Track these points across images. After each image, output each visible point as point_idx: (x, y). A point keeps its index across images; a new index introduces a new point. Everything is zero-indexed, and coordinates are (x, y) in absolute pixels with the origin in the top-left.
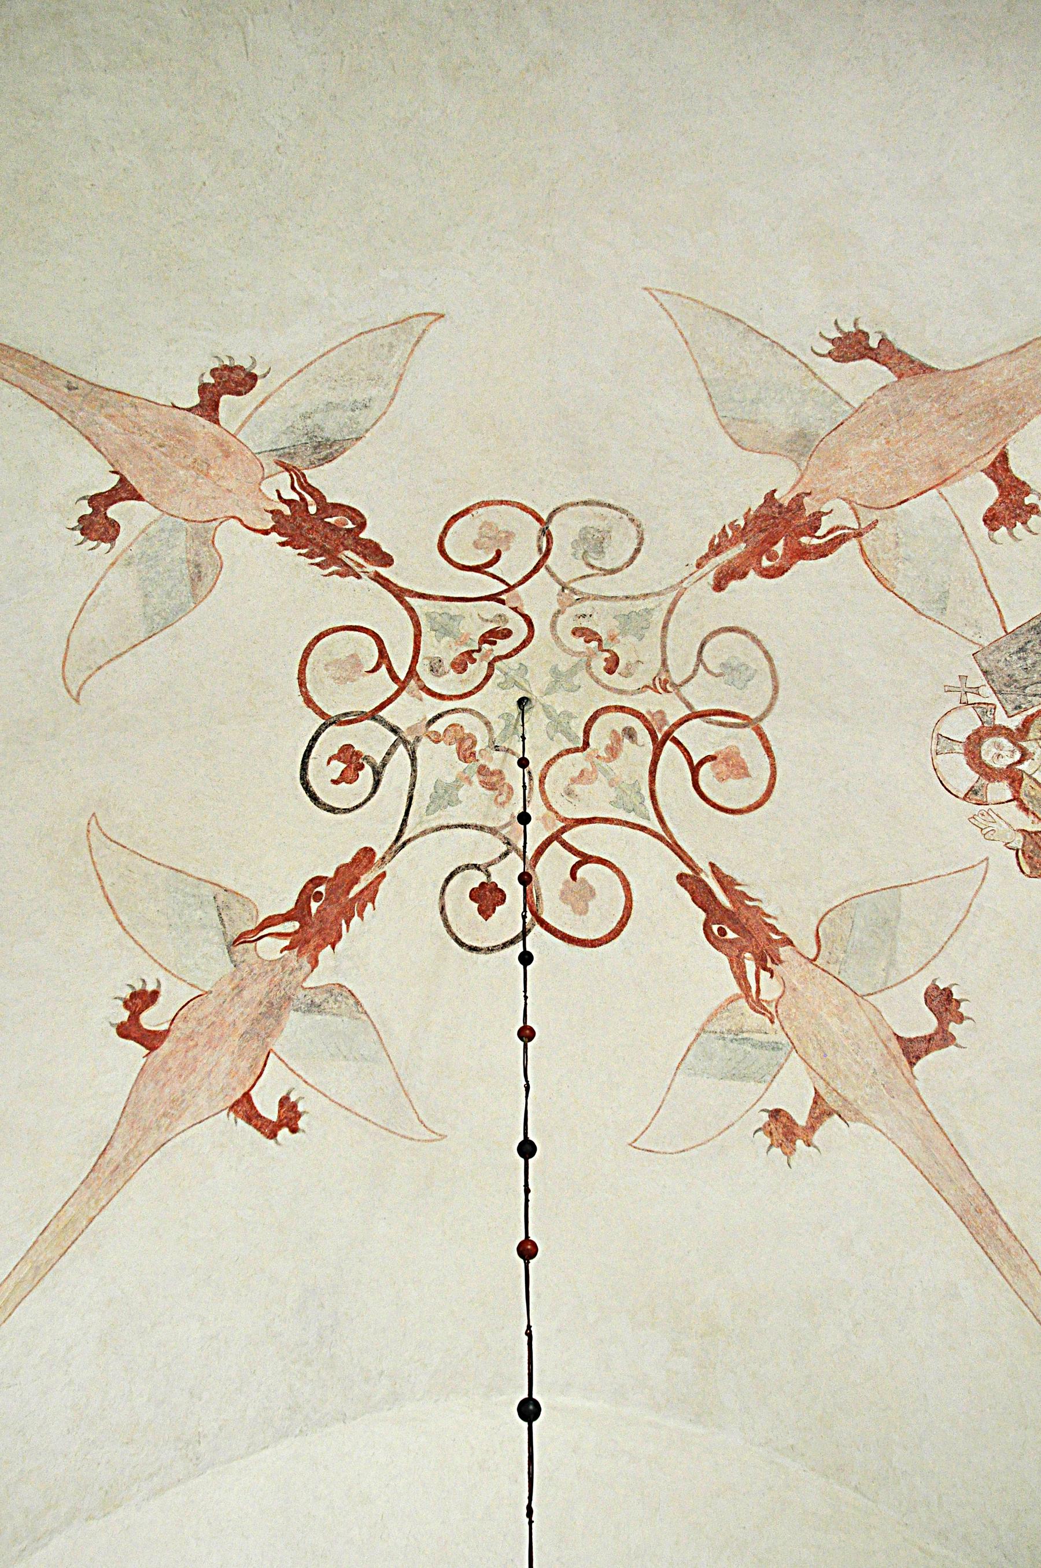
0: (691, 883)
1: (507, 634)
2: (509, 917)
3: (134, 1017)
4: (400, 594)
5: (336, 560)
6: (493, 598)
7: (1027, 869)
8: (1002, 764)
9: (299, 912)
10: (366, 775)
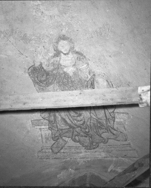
8: (60, 48)
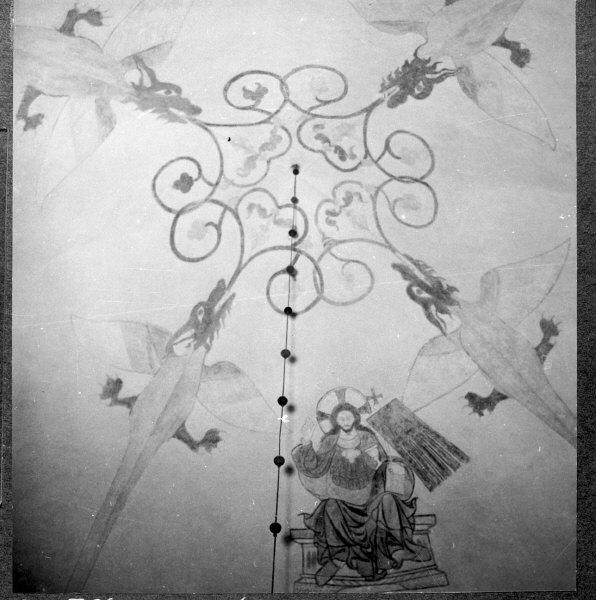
0: (220, 289)
1: (343, 157)
2: (177, 200)
3: (83, 16)
4: (369, 110)
5: (393, 82)
6: (367, 153)
7: (294, 452)
8: (340, 422)
9: (157, 84)
10: (250, 102)
